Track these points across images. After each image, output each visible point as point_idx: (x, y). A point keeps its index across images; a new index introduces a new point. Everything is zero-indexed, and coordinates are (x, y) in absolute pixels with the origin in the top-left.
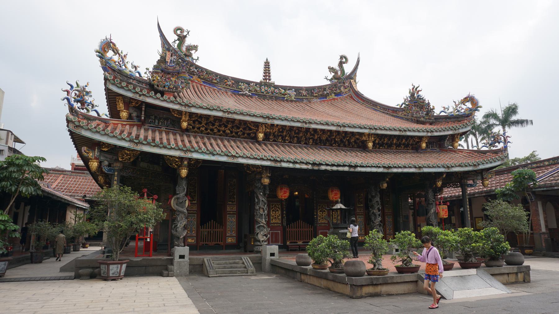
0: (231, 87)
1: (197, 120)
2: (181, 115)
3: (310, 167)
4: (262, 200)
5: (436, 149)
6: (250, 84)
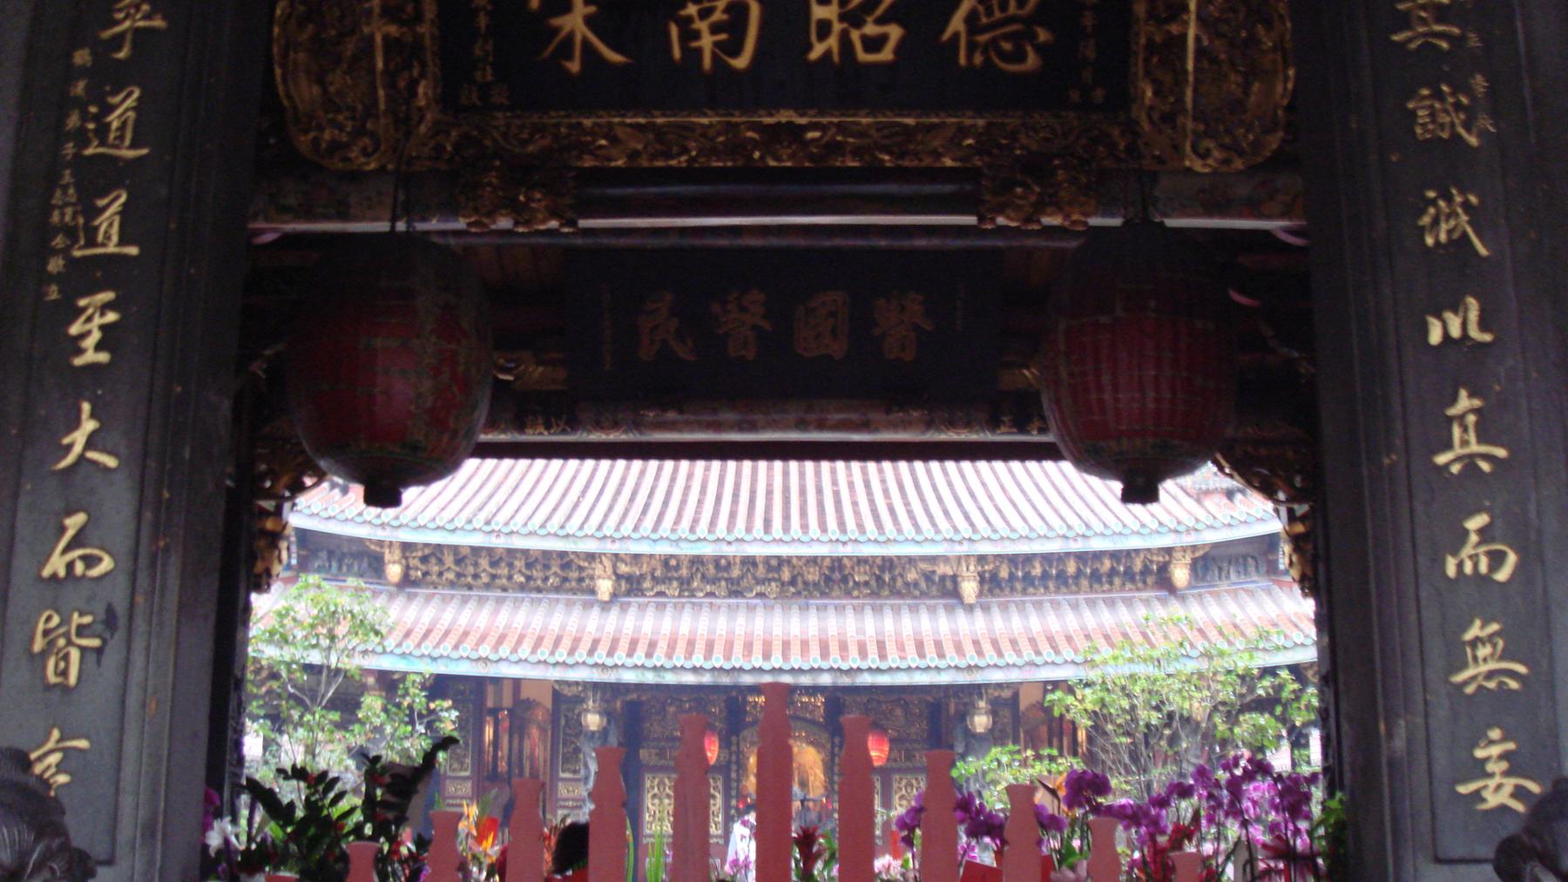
1: (433, 554)
2: (382, 547)
3: (706, 679)
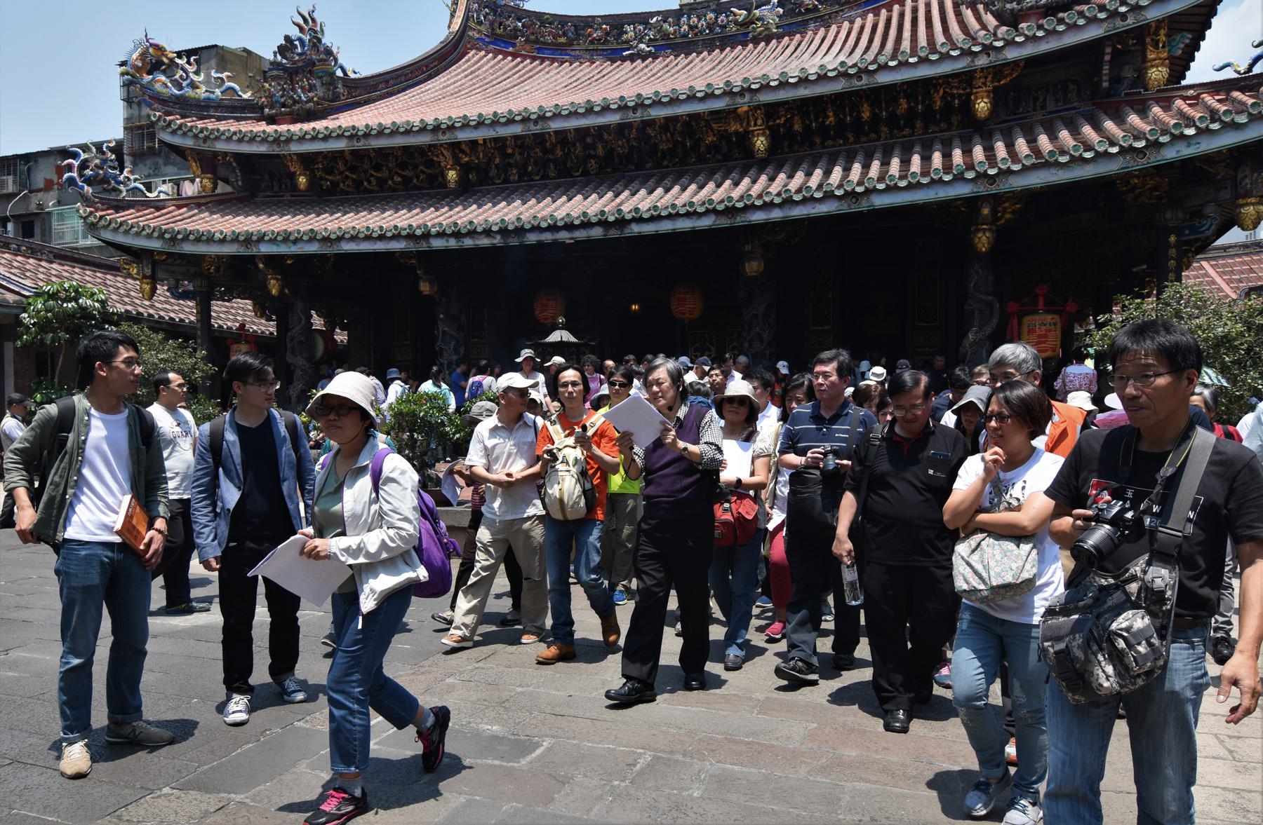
0: (603, 44)
4: (444, 332)
5: (1074, 108)
6: (648, 23)
